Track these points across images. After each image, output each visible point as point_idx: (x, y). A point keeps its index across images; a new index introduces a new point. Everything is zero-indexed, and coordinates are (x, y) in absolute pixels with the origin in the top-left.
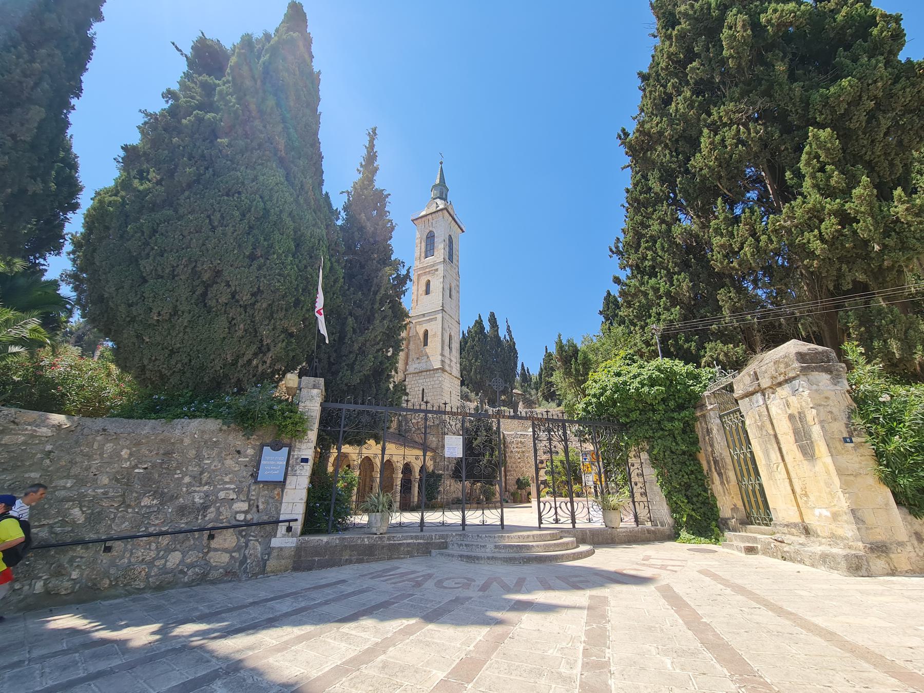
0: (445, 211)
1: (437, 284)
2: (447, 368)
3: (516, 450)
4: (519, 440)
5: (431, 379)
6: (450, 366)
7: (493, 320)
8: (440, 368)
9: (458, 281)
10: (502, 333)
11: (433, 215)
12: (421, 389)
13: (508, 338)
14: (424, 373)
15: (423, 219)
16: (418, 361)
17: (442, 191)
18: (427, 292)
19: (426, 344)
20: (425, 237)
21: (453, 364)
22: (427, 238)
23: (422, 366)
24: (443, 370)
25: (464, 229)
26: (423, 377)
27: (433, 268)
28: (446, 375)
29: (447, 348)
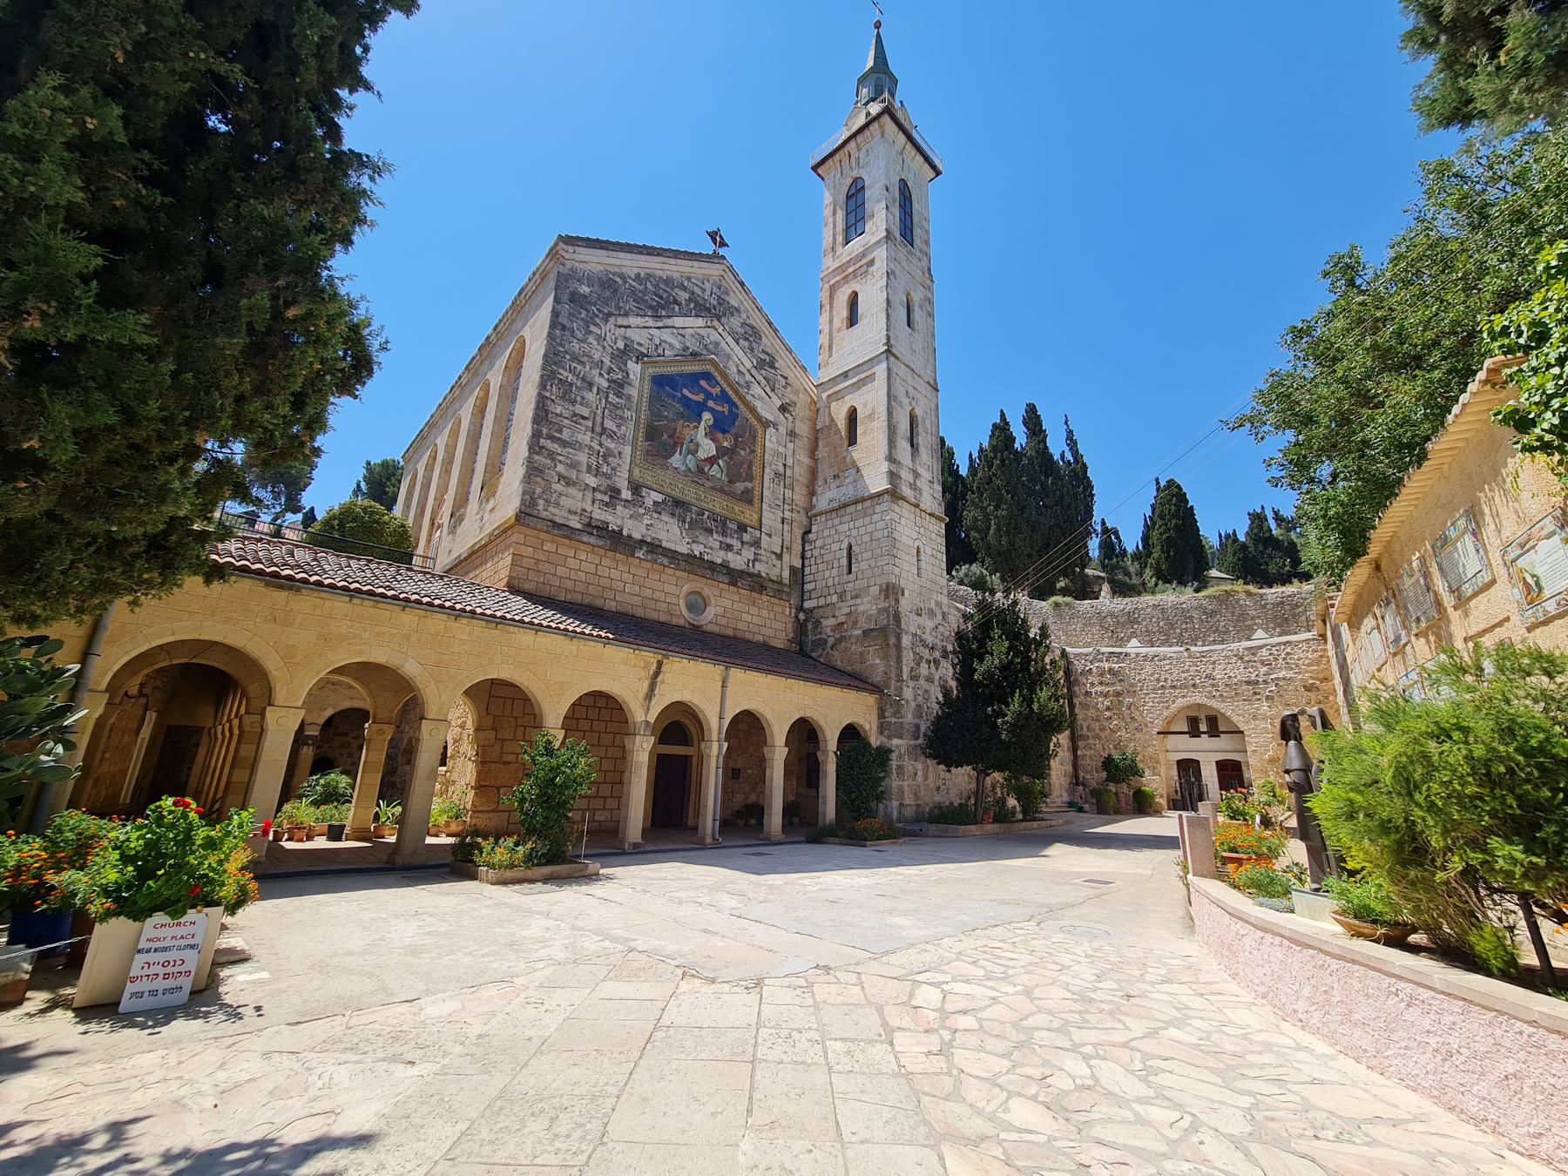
0: (886, 119)
1: (873, 294)
2: (906, 491)
3: (1099, 688)
4: (1107, 665)
5: (868, 520)
6: (913, 486)
7: (1033, 420)
8: (886, 492)
9: (929, 289)
10: (1056, 446)
11: (859, 138)
12: (845, 545)
13: (1069, 456)
14: (851, 509)
15: (837, 157)
16: (838, 482)
17: (881, 78)
18: (852, 320)
19: (852, 440)
20: (843, 197)
21: (922, 483)
22: (848, 197)
23: (846, 492)
24: (894, 494)
25: (940, 167)
26: (847, 518)
27: (864, 261)
28: (904, 510)
29: (903, 445)
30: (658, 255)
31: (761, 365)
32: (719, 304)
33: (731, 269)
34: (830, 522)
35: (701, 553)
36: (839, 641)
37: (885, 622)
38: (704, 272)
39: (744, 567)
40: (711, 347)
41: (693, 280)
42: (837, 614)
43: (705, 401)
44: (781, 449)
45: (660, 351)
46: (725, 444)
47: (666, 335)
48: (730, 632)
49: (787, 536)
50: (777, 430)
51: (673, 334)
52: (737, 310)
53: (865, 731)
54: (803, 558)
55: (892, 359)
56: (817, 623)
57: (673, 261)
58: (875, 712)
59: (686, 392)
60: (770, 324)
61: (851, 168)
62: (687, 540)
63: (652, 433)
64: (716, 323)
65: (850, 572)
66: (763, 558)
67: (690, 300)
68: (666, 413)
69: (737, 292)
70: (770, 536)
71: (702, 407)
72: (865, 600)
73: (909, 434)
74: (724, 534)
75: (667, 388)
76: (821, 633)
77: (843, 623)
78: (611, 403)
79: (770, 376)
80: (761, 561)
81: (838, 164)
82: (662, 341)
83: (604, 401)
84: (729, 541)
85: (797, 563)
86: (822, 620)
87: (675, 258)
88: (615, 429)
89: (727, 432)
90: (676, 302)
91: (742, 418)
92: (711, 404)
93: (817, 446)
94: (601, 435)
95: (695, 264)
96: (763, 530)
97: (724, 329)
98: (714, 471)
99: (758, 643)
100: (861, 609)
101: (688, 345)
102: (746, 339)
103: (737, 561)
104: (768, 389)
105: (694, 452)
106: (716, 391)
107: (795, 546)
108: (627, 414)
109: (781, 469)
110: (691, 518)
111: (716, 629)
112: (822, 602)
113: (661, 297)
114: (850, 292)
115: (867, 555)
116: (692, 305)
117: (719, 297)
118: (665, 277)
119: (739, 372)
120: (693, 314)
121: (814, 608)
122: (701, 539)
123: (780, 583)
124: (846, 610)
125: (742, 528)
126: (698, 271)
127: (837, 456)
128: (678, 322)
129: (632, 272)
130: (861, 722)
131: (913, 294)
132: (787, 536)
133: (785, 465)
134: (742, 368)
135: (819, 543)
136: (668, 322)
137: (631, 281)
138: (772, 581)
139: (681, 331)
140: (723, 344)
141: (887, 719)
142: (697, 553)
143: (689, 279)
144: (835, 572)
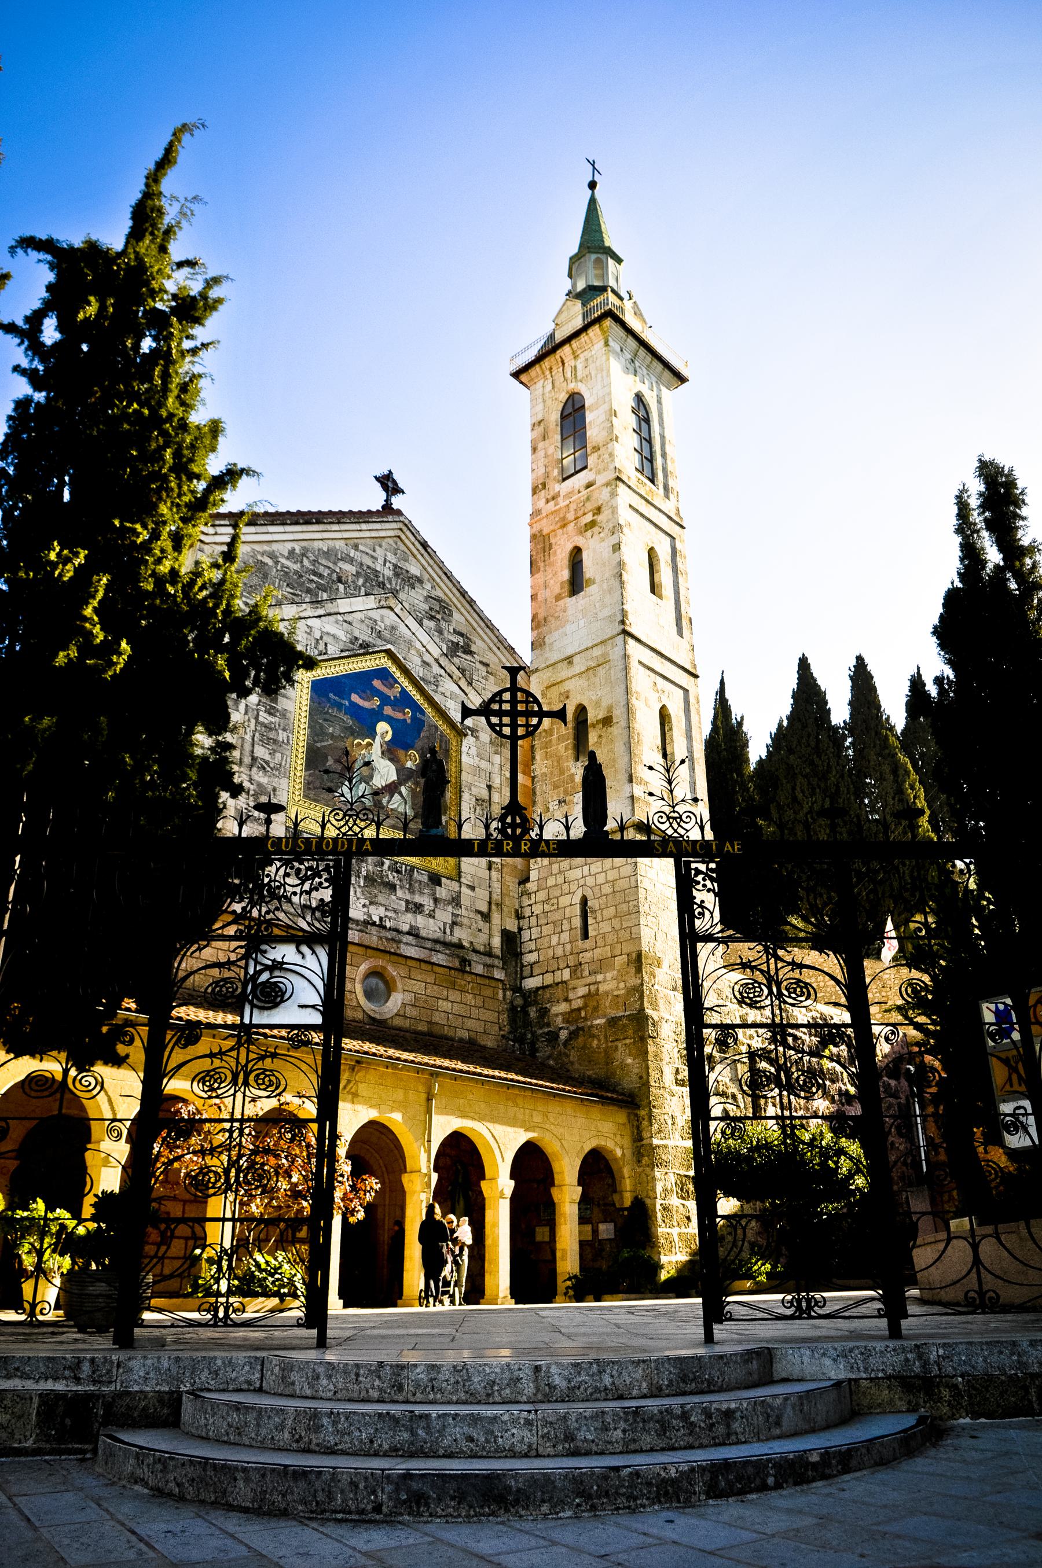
11: (575, 343)
12: (577, 899)
15: (546, 363)
18: (576, 584)
20: (555, 416)
22: (563, 417)
30: (318, 522)
31: (454, 650)
32: (397, 575)
33: (408, 526)
34: (555, 867)
35: (381, 919)
36: (573, 1035)
37: (637, 1005)
38: (374, 534)
39: (439, 935)
40: (386, 634)
41: (361, 548)
42: (571, 996)
43: (381, 707)
44: (484, 764)
45: (321, 647)
46: (409, 764)
47: (329, 626)
48: (422, 1027)
49: (496, 885)
50: (477, 738)
51: (337, 622)
52: (420, 581)
53: (616, 1159)
54: (519, 916)
55: (631, 642)
56: (544, 1012)
57: (335, 527)
58: (627, 1132)
59: (355, 698)
60: (463, 593)
61: (566, 379)
62: (363, 901)
63: (314, 758)
64: (392, 602)
65: (585, 936)
66: (465, 921)
67: (358, 575)
68: (331, 730)
69: (419, 557)
70: (472, 888)
71: (377, 715)
72: (609, 975)
73: (659, 742)
74: (411, 890)
75: (331, 695)
76: (548, 1025)
77: (579, 1010)
78: (263, 724)
79: (465, 665)
80: (461, 925)
81: (548, 373)
82: (324, 634)
83: (253, 721)
84: (417, 899)
85: (512, 925)
86: (548, 1006)
87: (339, 523)
88: (267, 757)
89: (412, 748)
90: (340, 580)
91: (430, 726)
92: (388, 710)
93: (533, 758)
94: (251, 767)
95: (364, 526)
96: (463, 880)
97: (403, 608)
98: (395, 803)
99: (461, 1040)
100: (603, 988)
101: (357, 634)
102: (432, 618)
103: (430, 927)
104: (463, 683)
105: (367, 780)
106: (394, 693)
107: (507, 901)
108: (282, 736)
109: (484, 794)
110: (368, 871)
111: (406, 1024)
112: (549, 979)
113: (321, 576)
114: (569, 547)
115: (610, 912)
116: (361, 581)
117: (395, 566)
118: (325, 549)
119: (425, 664)
120: (363, 589)
121: (538, 989)
122: (381, 899)
123: (489, 954)
124: (582, 991)
125: (435, 879)
126: (368, 534)
127: (562, 772)
128: (343, 605)
129: (284, 549)
130: (610, 1144)
131: (656, 548)
132: (496, 885)
133: (489, 787)
134: (427, 658)
135: (542, 896)
136: (330, 607)
137: (283, 560)
138: (475, 951)
139: (348, 618)
140: (402, 628)
141: (644, 1142)
142: (376, 919)
143: (356, 547)
144: (565, 937)
